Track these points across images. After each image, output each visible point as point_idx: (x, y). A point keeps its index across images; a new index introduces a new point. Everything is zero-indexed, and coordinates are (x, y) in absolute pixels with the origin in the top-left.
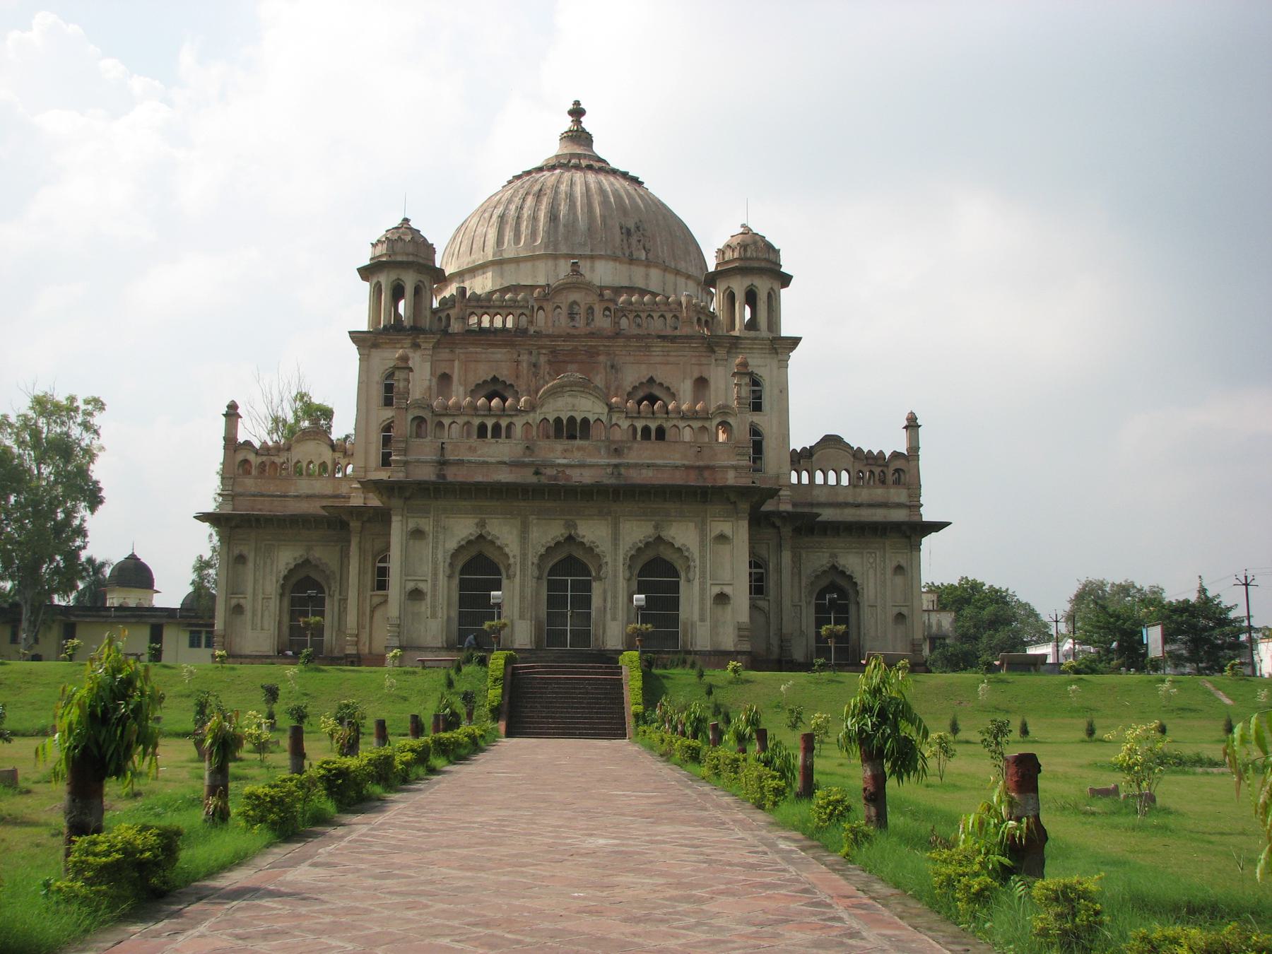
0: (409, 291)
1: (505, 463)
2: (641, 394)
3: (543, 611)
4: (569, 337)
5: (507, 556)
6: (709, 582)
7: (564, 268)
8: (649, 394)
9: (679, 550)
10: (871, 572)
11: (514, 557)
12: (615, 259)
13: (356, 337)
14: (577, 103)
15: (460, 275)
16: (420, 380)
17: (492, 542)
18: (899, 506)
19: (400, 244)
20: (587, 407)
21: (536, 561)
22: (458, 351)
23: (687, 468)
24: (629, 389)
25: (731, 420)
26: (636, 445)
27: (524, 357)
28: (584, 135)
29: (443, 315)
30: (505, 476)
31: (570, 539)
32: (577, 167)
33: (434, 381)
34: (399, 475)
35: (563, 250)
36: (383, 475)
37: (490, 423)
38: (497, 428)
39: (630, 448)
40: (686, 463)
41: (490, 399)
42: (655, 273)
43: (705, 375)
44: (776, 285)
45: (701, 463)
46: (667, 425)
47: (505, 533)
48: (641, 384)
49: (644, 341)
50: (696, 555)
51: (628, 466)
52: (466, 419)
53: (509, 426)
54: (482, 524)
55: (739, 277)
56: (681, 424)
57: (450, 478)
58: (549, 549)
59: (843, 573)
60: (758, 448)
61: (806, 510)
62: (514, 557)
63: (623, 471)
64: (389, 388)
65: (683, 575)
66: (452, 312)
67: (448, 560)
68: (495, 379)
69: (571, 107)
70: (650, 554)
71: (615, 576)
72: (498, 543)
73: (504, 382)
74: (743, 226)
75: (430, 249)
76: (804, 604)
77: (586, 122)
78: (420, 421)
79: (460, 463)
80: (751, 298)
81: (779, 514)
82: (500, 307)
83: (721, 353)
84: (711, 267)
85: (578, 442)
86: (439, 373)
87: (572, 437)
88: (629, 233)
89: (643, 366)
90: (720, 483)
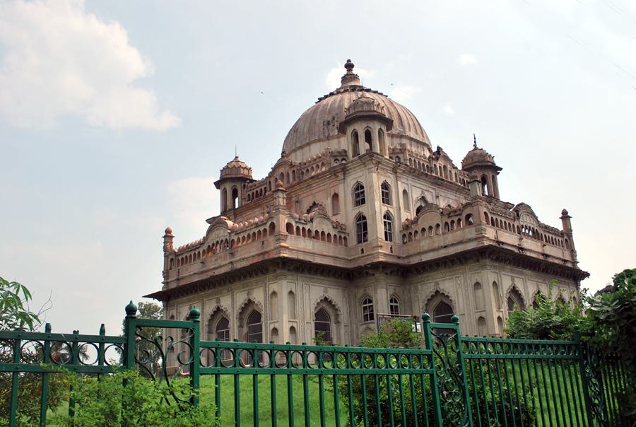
1: (195, 274)
6: (269, 322)
12: (319, 140)
14: (349, 61)
18: (470, 240)
30: (196, 279)
40: (257, 252)
51: (236, 261)
58: (212, 316)
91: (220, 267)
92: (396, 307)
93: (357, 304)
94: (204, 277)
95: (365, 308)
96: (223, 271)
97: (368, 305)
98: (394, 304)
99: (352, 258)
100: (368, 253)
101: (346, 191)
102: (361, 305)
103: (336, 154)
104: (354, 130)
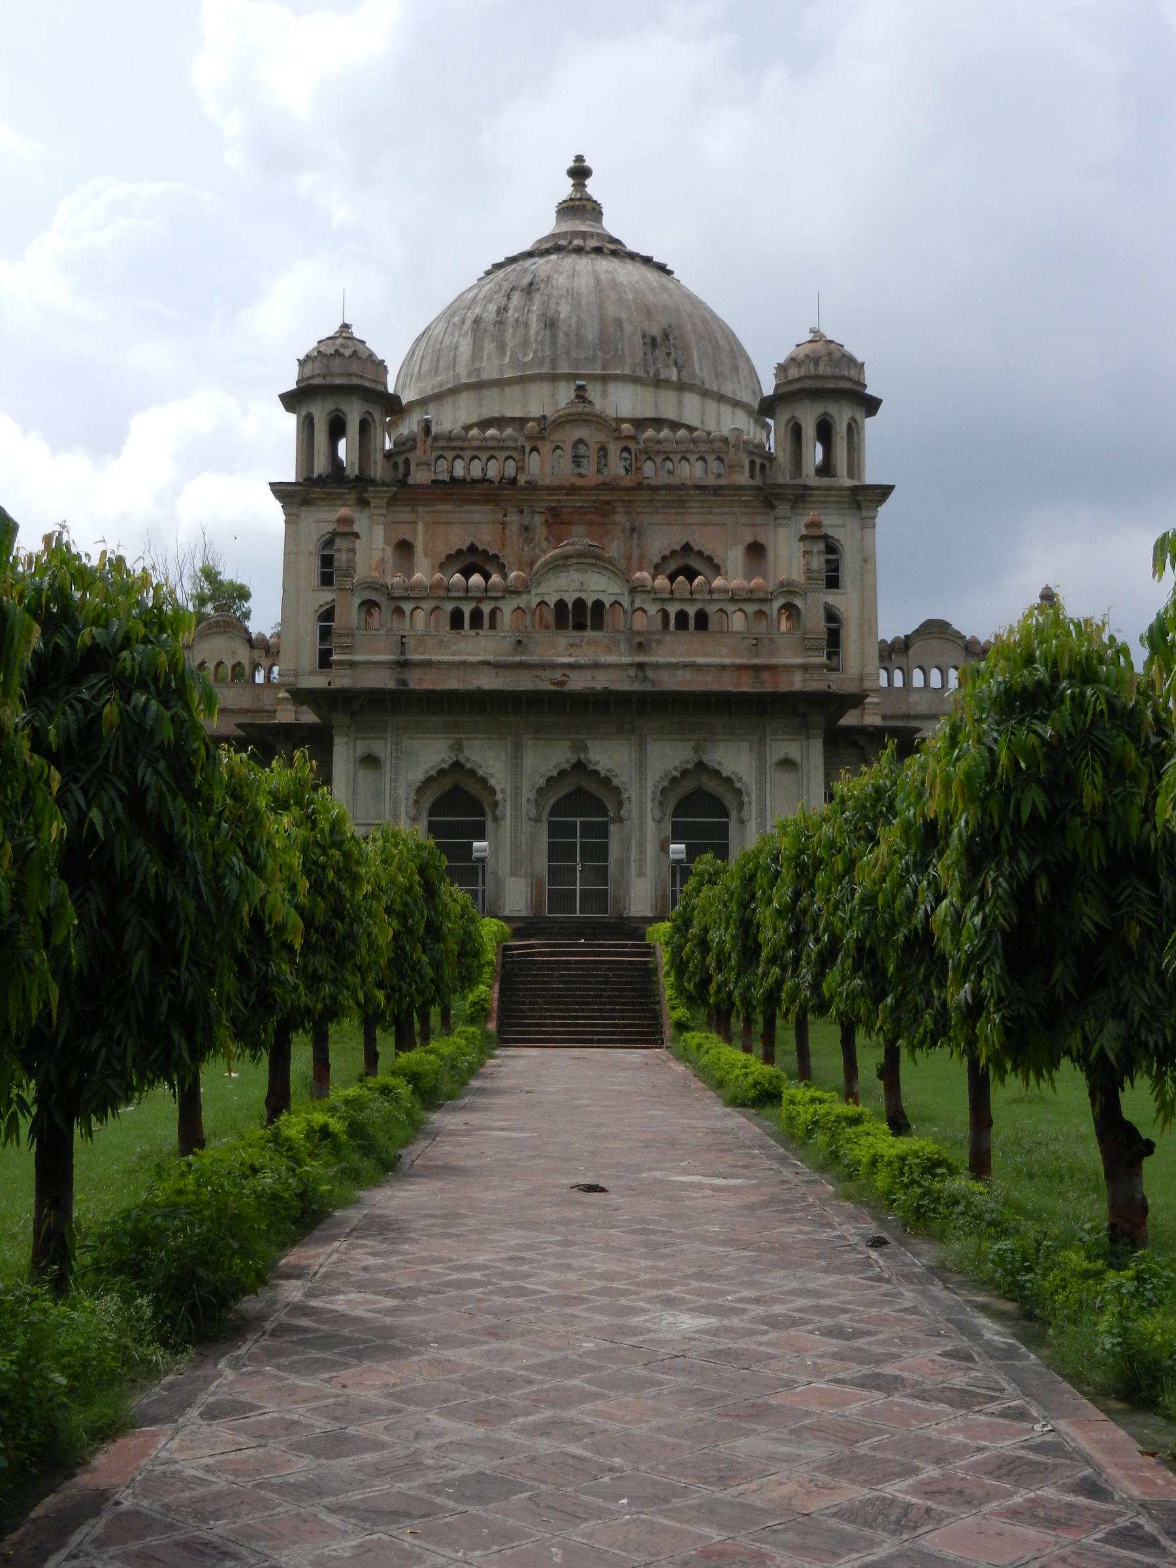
0: (353, 426)
1: (488, 663)
2: (673, 566)
3: (542, 864)
4: (572, 489)
5: (493, 791)
7: (565, 394)
8: (686, 564)
9: (728, 781)
11: (503, 791)
12: (635, 380)
13: (279, 490)
14: (579, 159)
15: (423, 402)
16: (371, 549)
17: (472, 772)
19: (337, 361)
20: (599, 586)
21: (532, 795)
22: (420, 509)
23: (740, 668)
24: (657, 560)
25: (798, 602)
26: (668, 638)
27: (513, 518)
28: (589, 205)
29: (400, 460)
30: (487, 682)
31: (580, 767)
32: (579, 250)
33: (389, 552)
34: (341, 680)
35: (564, 368)
36: (318, 682)
37: (467, 608)
38: (477, 615)
39: (659, 642)
40: (737, 661)
41: (467, 574)
42: (691, 401)
43: (761, 539)
44: (858, 416)
45: (758, 661)
46: (711, 609)
47: (489, 759)
48: (673, 552)
49: (678, 496)
50: (753, 788)
51: (658, 667)
52: (434, 603)
53: (493, 613)
54: (458, 747)
55: (808, 403)
56: (730, 608)
57: (414, 685)
58: (550, 780)
60: (834, 640)
61: (900, 723)
62: (503, 791)
63: (650, 674)
64: (327, 561)
65: (734, 813)
66: (412, 457)
67: (413, 796)
68: (472, 548)
69: (572, 164)
70: (689, 786)
71: (642, 817)
72: (480, 772)
73: (485, 552)
74: (811, 331)
75: (381, 367)
77: (593, 188)
78: (369, 605)
79: (427, 664)
80: (825, 432)
81: (862, 730)
82: (479, 448)
83: (783, 509)
84: (768, 389)
85: (589, 634)
86: (396, 539)
87: (580, 626)
88: (654, 341)
89: (676, 529)
90: (784, 688)
91: (596, 666)
94: (525, 682)
96: (601, 681)
103: (751, 448)
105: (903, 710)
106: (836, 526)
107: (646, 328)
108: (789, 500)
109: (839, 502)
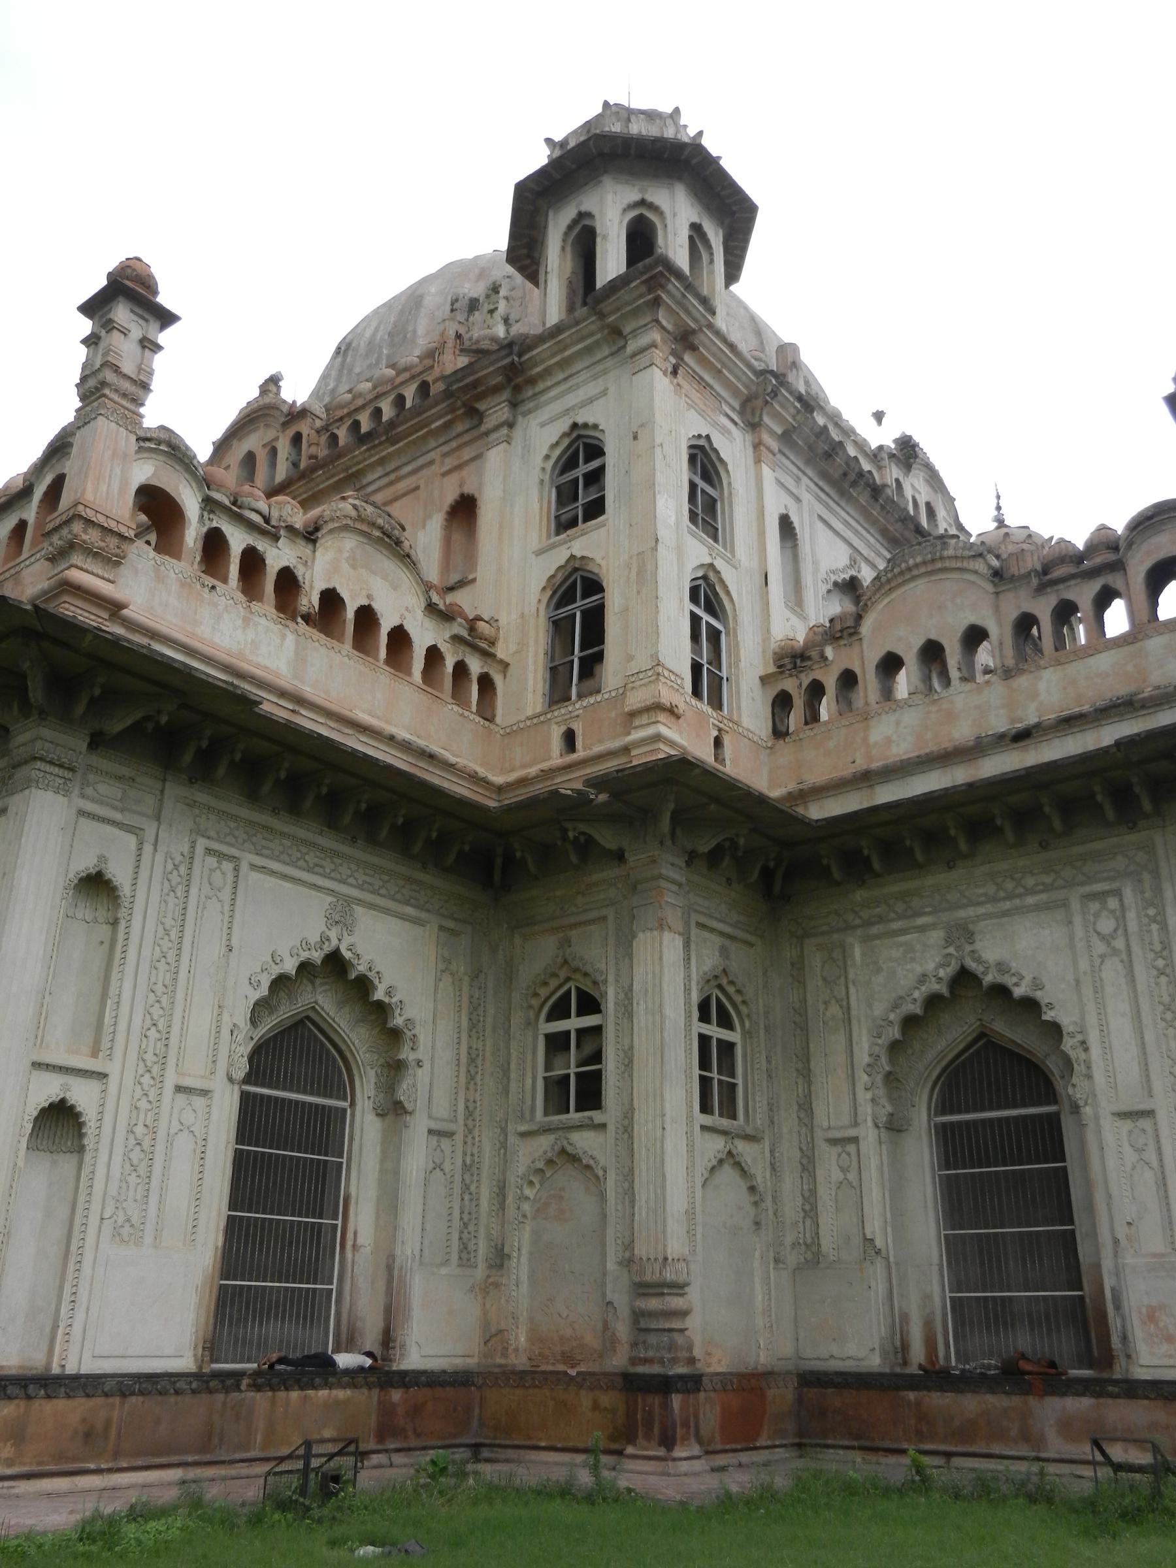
10: (1112, 972)
43: (468, 489)
59: (1001, 991)
76: (869, 1135)
83: (497, 411)
92: (727, 1048)
93: (517, 1018)
95: (557, 1044)
97: (574, 1023)
98: (714, 1031)
99: (512, 777)
100: (598, 749)
101: (513, 475)
102: (531, 1024)
104: (582, 215)
105: (861, 764)
106: (591, 401)
107: (461, 291)
108: (497, 389)
109: (588, 350)
